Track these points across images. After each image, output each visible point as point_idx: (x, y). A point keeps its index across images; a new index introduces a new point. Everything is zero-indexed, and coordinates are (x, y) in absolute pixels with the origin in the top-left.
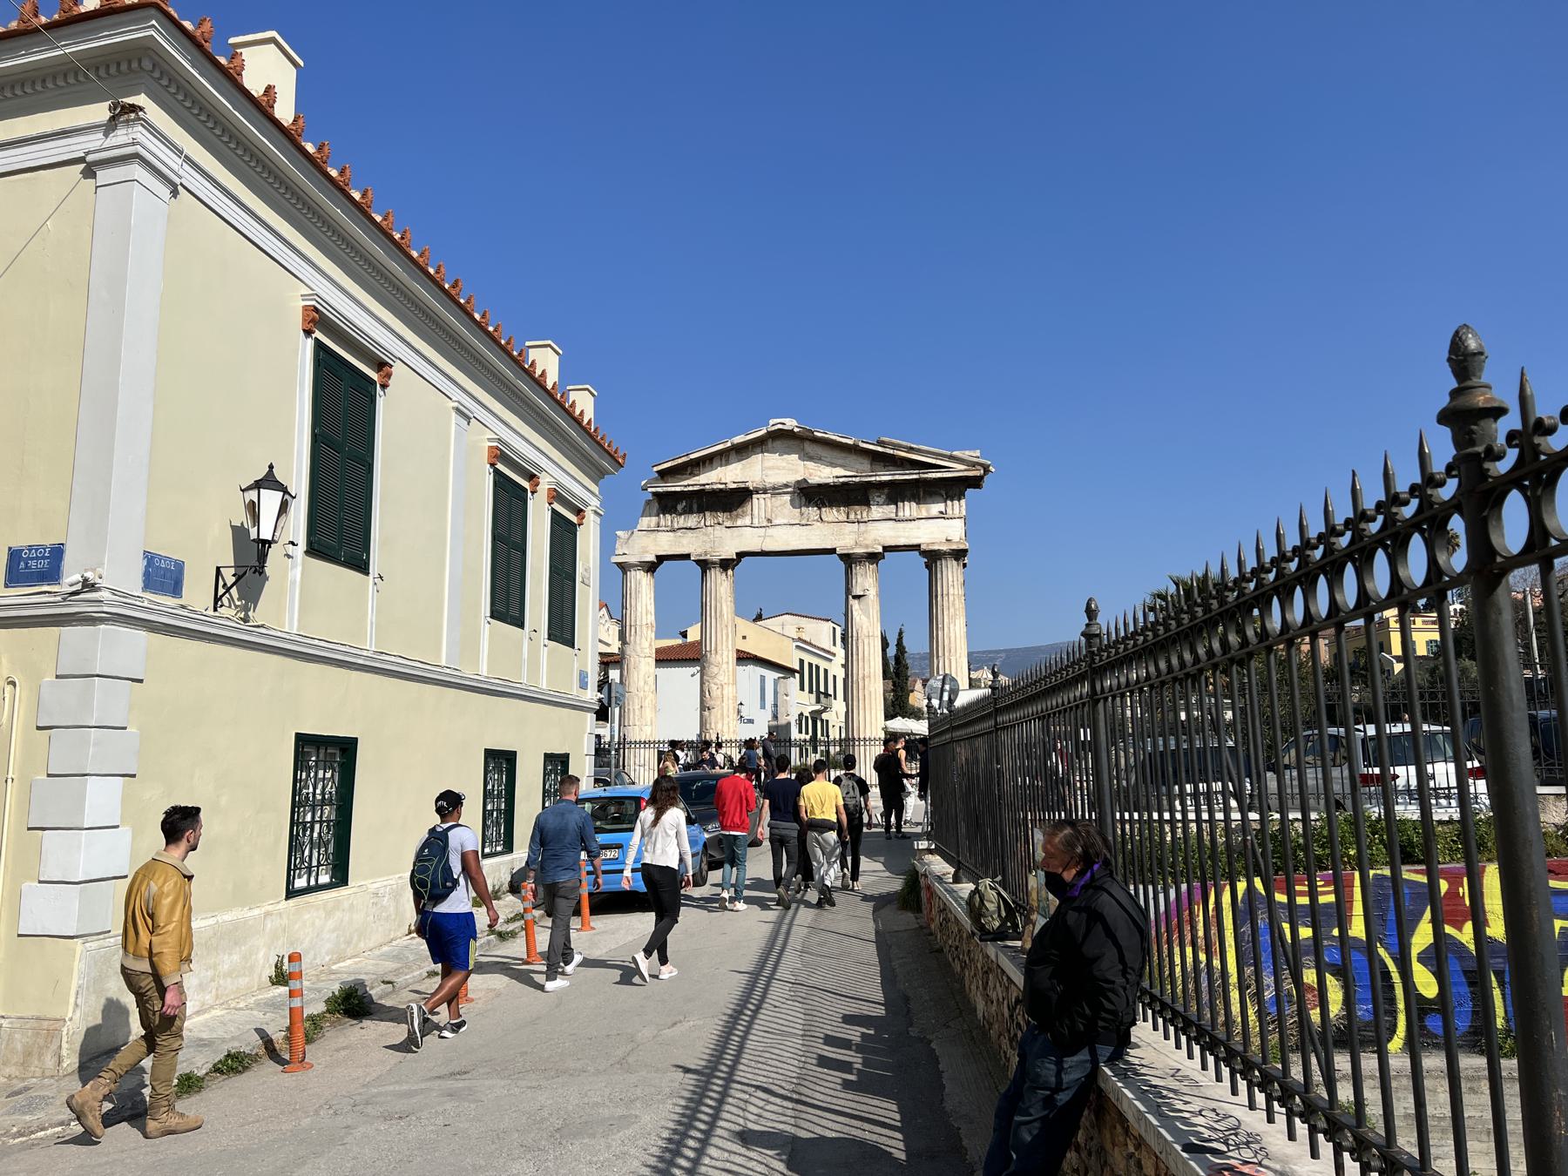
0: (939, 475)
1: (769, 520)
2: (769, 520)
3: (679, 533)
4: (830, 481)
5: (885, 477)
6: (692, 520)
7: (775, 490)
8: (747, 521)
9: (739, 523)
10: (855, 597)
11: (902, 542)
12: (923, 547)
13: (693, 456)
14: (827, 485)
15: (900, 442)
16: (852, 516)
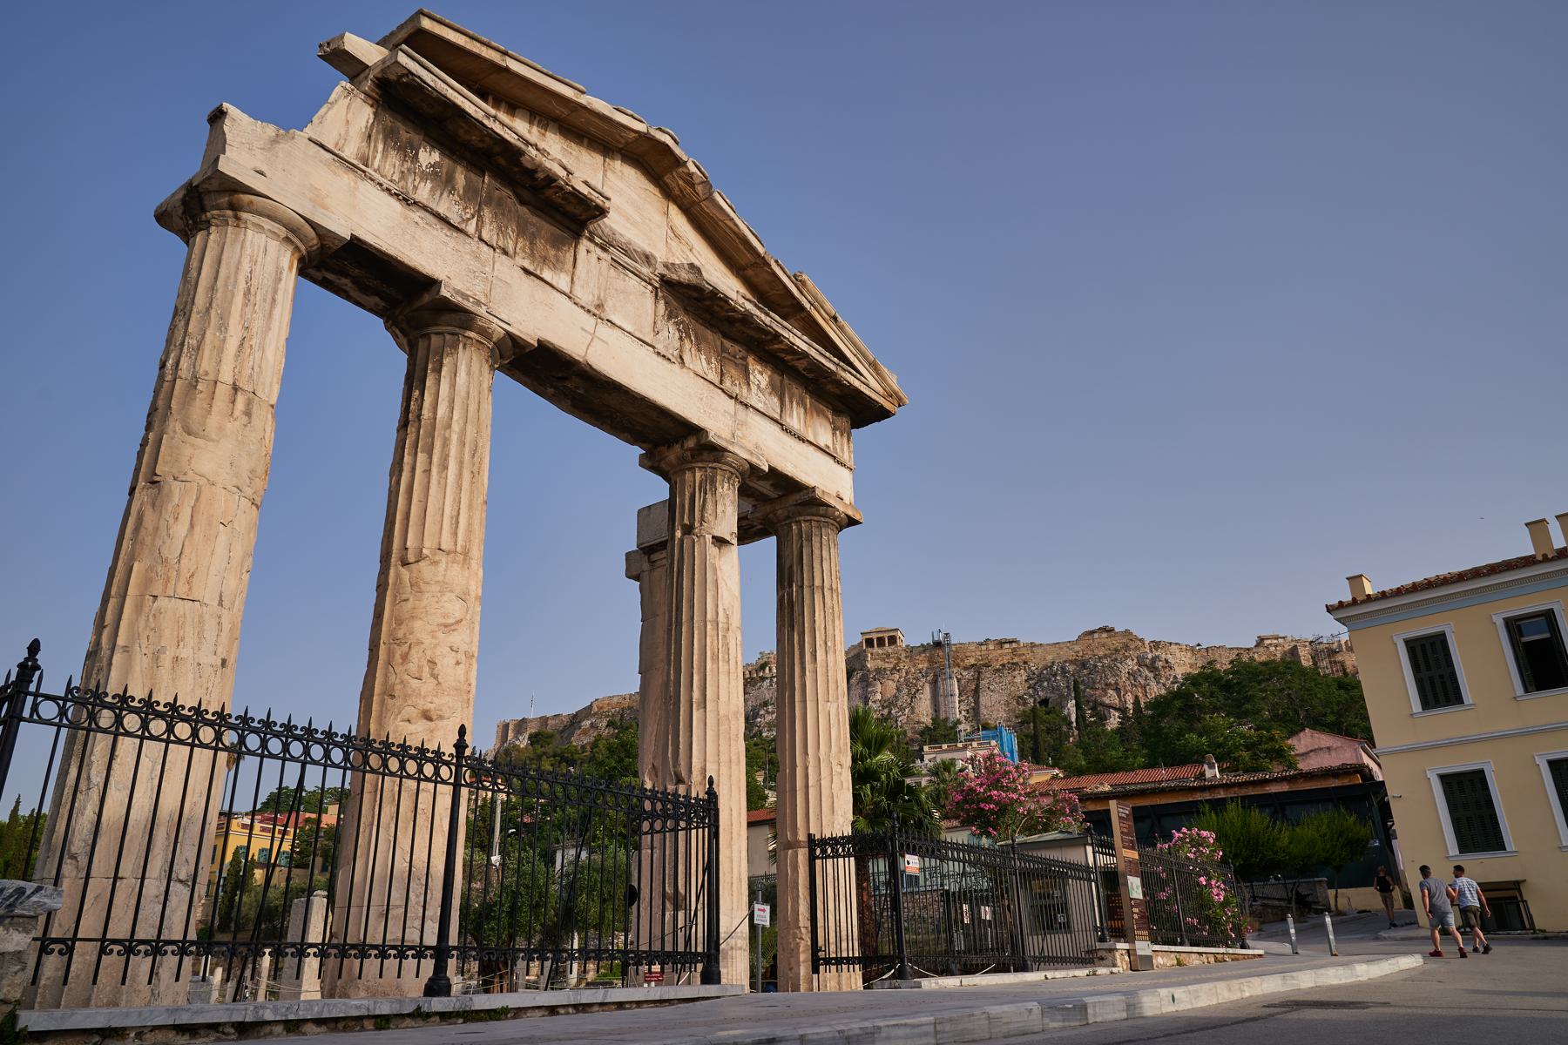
0: (857, 383)
1: (600, 306)
2: (600, 306)
3: (417, 215)
4: (733, 295)
5: (800, 342)
6: (447, 206)
7: (625, 257)
8: (562, 281)
9: (547, 275)
10: (720, 542)
11: (788, 468)
12: (818, 493)
13: (515, 66)
14: (726, 300)
15: (820, 297)
16: (727, 384)
